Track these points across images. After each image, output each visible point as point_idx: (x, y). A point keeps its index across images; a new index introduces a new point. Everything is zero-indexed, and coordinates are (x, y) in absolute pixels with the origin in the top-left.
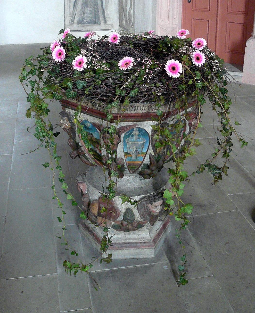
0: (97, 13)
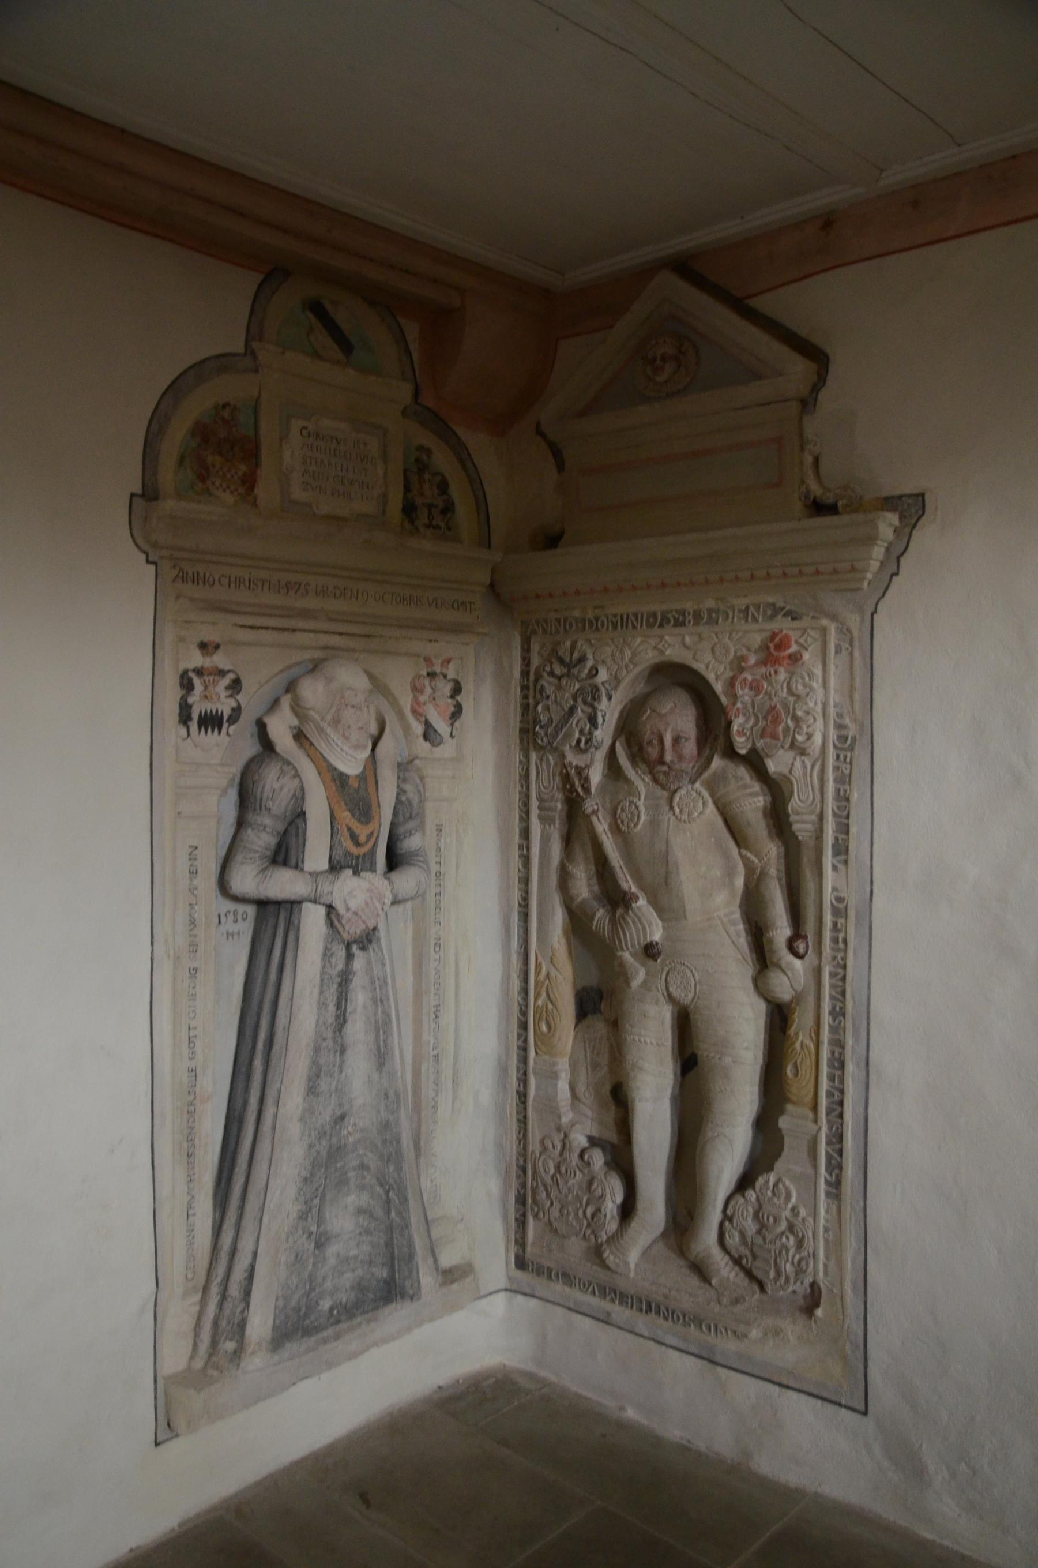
0: (399, 1214)
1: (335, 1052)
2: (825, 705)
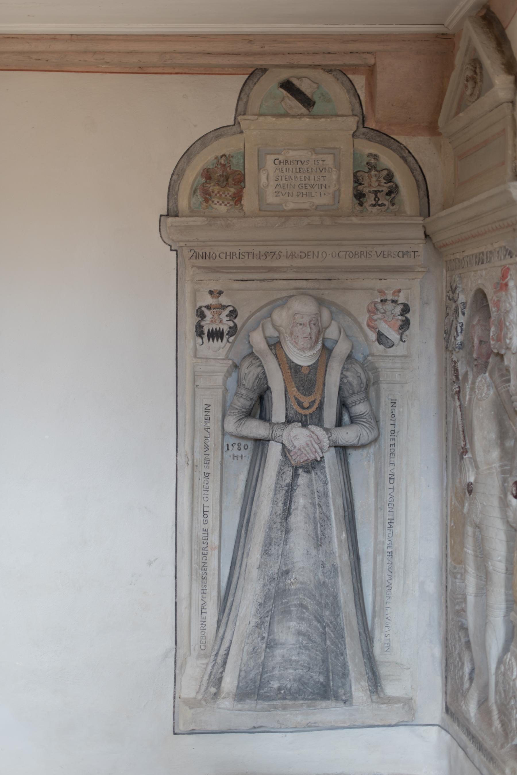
1: (282, 531)
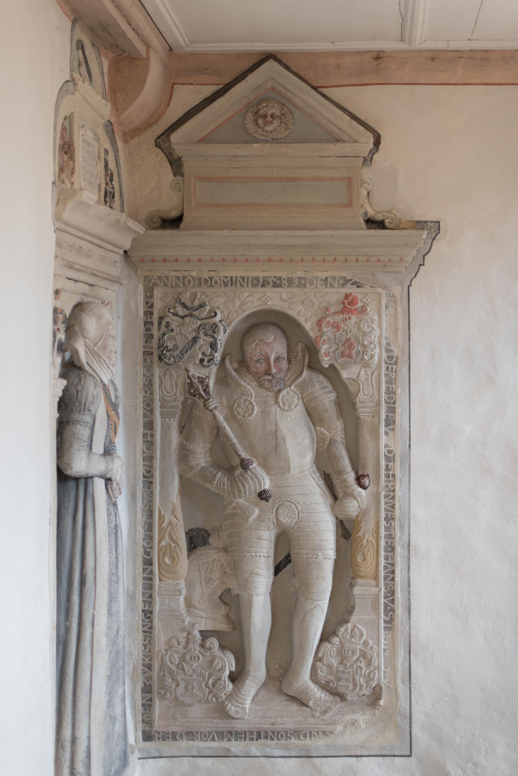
2: (380, 338)
